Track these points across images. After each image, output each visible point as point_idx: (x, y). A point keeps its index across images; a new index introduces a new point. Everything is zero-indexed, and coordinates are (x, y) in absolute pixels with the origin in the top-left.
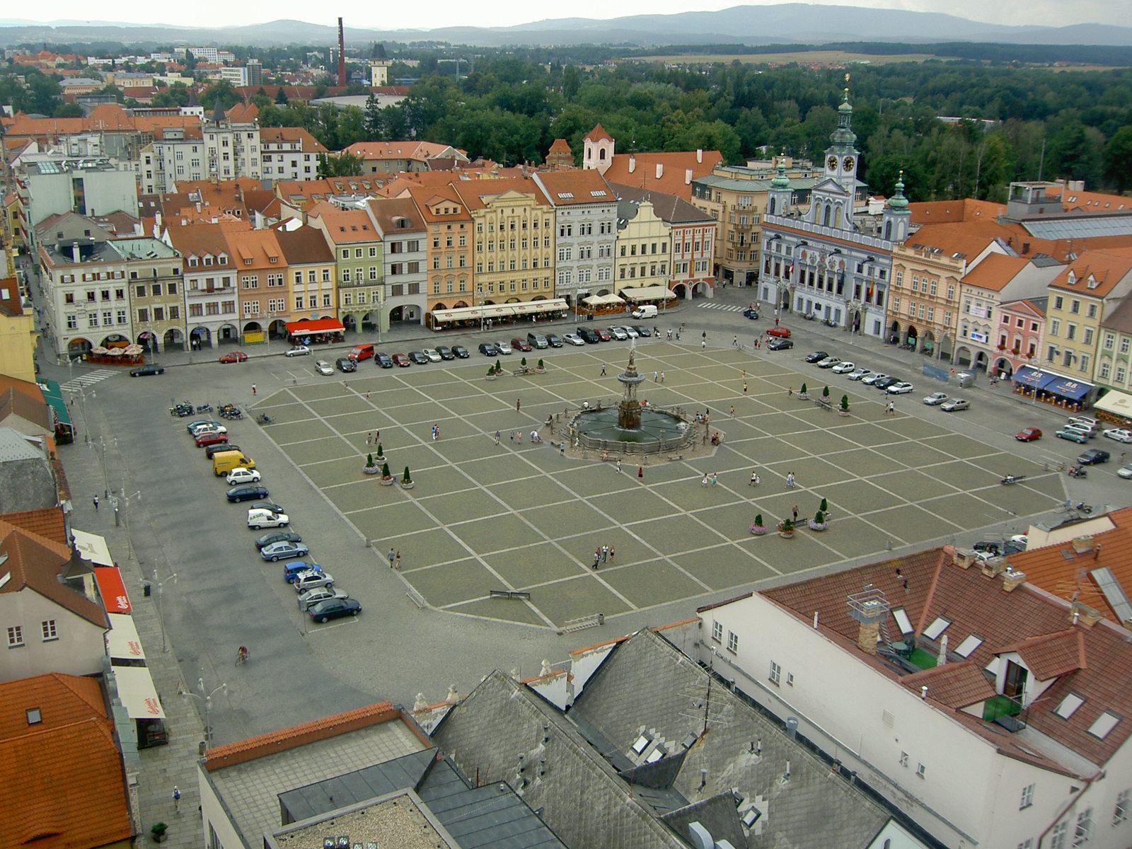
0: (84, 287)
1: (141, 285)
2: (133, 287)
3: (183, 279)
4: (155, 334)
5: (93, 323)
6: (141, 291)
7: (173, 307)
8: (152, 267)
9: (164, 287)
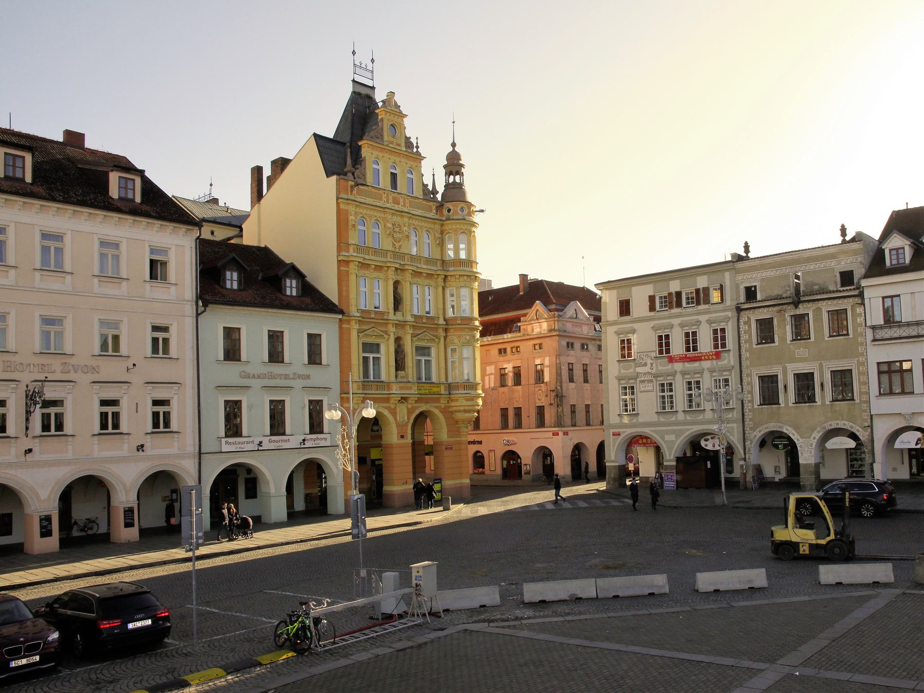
0: (652, 323)
1: (764, 314)
2: (748, 323)
3: (861, 295)
4: (795, 437)
5: (666, 403)
6: (766, 330)
7: (843, 372)
8: (789, 270)
9: (818, 319)
